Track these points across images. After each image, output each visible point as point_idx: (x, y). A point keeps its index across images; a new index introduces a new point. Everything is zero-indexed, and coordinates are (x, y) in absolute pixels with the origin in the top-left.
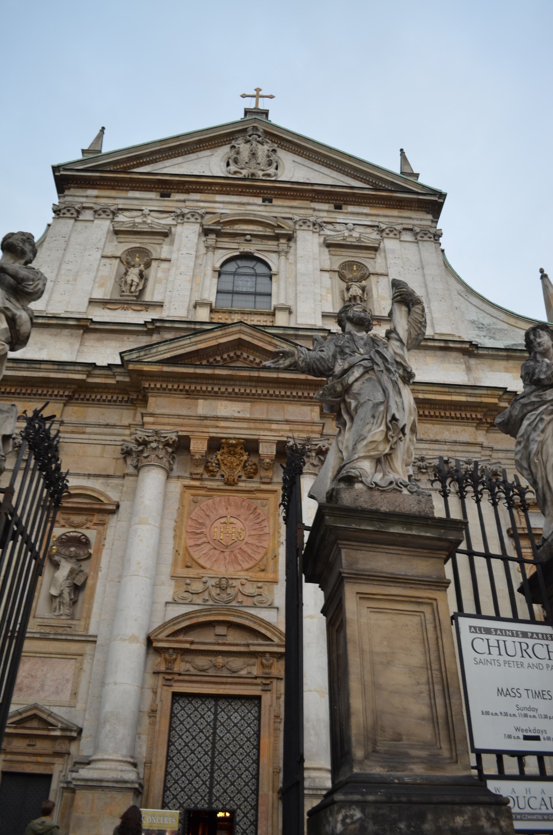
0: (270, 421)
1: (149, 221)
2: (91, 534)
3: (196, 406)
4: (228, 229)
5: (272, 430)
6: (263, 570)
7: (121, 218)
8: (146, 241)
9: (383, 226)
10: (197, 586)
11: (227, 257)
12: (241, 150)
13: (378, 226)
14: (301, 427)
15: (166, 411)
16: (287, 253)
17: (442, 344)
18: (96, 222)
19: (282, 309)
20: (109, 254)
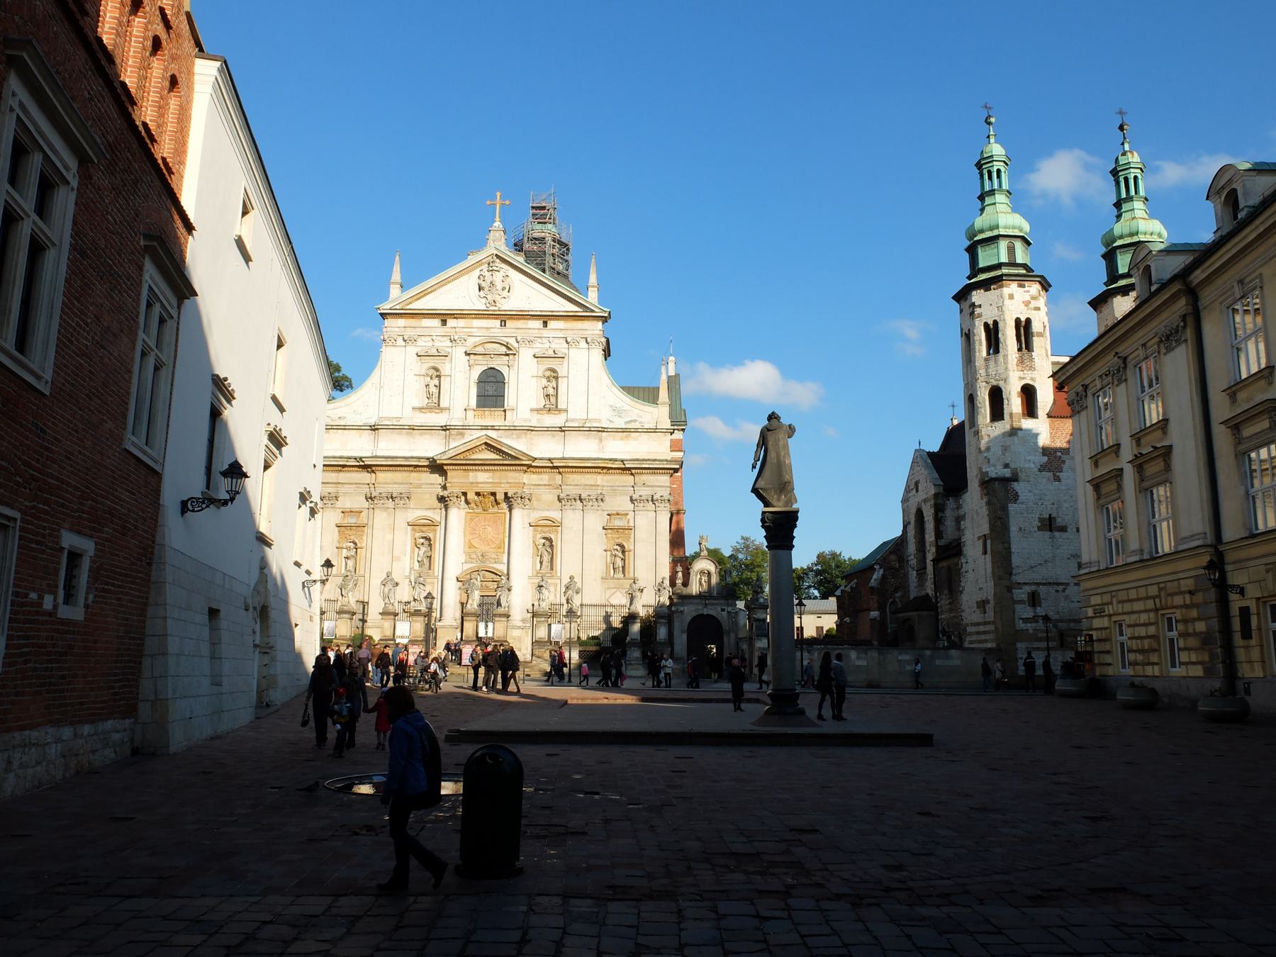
0: (501, 483)
1: (437, 344)
2: (431, 535)
3: (469, 476)
4: (480, 350)
5: (501, 487)
6: (499, 548)
7: (420, 342)
8: (436, 361)
9: (569, 339)
10: (474, 556)
12: (486, 278)
13: (566, 338)
14: (514, 485)
15: (456, 480)
16: (513, 366)
17: (588, 429)
19: (509, 410)
20: (418, 373)
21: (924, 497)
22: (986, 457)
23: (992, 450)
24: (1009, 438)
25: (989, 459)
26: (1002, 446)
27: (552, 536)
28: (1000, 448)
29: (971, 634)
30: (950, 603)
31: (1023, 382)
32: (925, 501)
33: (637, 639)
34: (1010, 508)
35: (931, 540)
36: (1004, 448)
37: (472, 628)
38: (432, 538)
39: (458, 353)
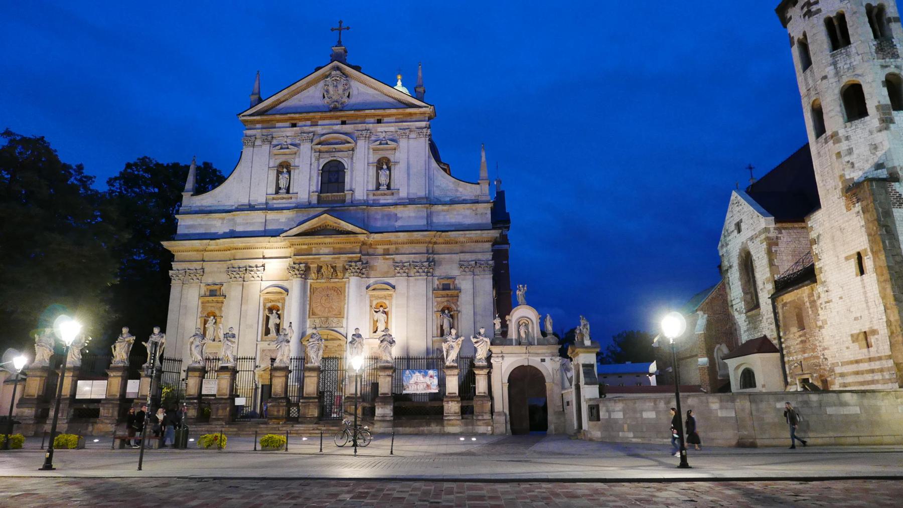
11: (325, 162)
18: (264, 147)
21: (750, 234)
22: (848, 162)
23: (856, 152)
24: (879, 134)
25: (853, 164)
26: (871, 144)
27: (387, 302)
28: (868, 148)
29: (842, 375)
30: (802, 342)
31: (887, 71)
32: (752, 239)
33: (455, 393)
34: (894, 214)
35: (764, 277)
36: (873, 147)
37: (280, 385)
38: (281, 307)
39: (306, 148)
